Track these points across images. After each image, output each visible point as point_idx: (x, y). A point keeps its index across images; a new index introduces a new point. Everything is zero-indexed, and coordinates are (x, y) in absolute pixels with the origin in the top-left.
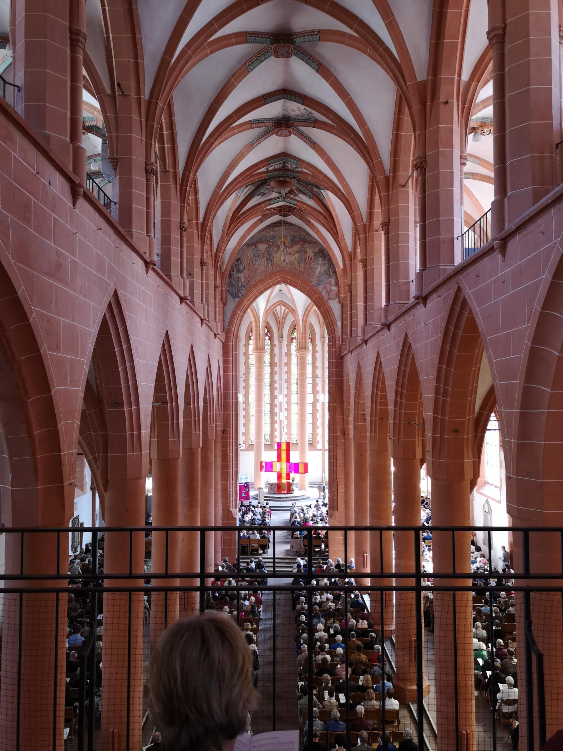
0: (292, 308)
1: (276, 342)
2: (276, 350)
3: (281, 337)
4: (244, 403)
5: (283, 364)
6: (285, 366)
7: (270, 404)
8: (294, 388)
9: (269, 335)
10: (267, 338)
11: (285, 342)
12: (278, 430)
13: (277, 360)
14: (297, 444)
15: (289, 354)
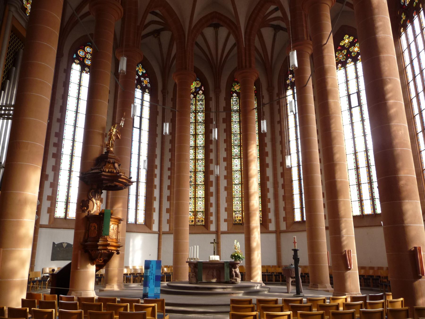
0: (230, 20)
1: (212, 95)
2: (212, 104)
3: (217, 88)
4: (169, 169)
5: (221, 121)
6: (224, 122)
7: (204, 172)
8: (236, 151)
9: (203, 88)
10: (201, 92)
11: (223, 95)
12: (214, 205)
13: (213, 116)
14: (241, 224)
15: (228, 110)
